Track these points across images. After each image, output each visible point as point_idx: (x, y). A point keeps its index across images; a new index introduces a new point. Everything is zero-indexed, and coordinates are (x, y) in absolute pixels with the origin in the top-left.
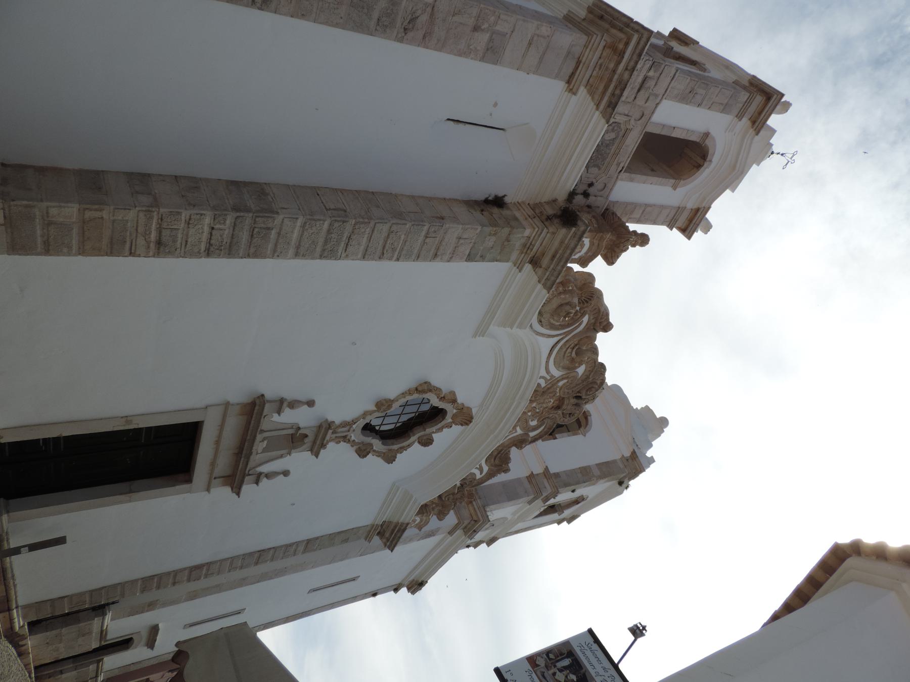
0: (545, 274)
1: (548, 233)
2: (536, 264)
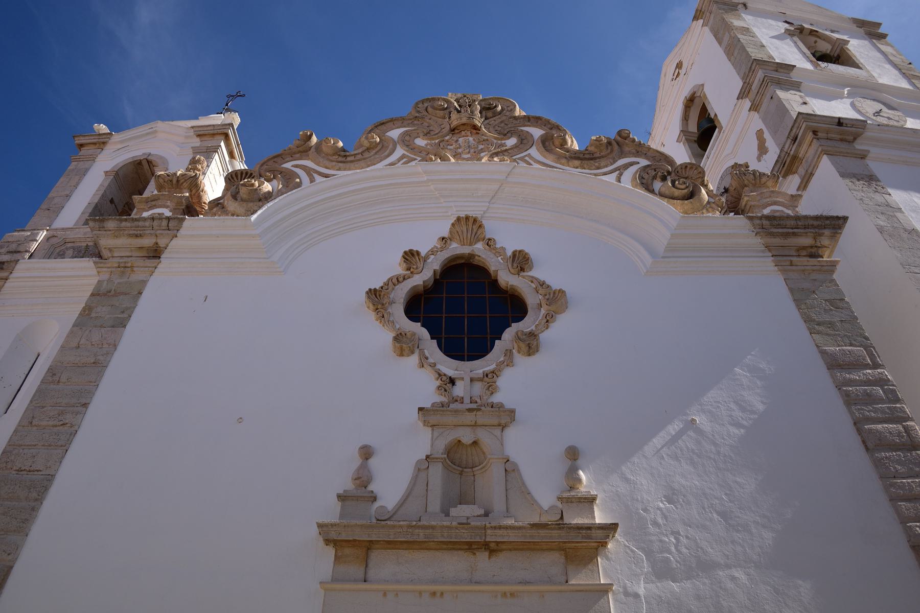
0: (162, 234)
1: (113, 257)
2: (156, 250)
